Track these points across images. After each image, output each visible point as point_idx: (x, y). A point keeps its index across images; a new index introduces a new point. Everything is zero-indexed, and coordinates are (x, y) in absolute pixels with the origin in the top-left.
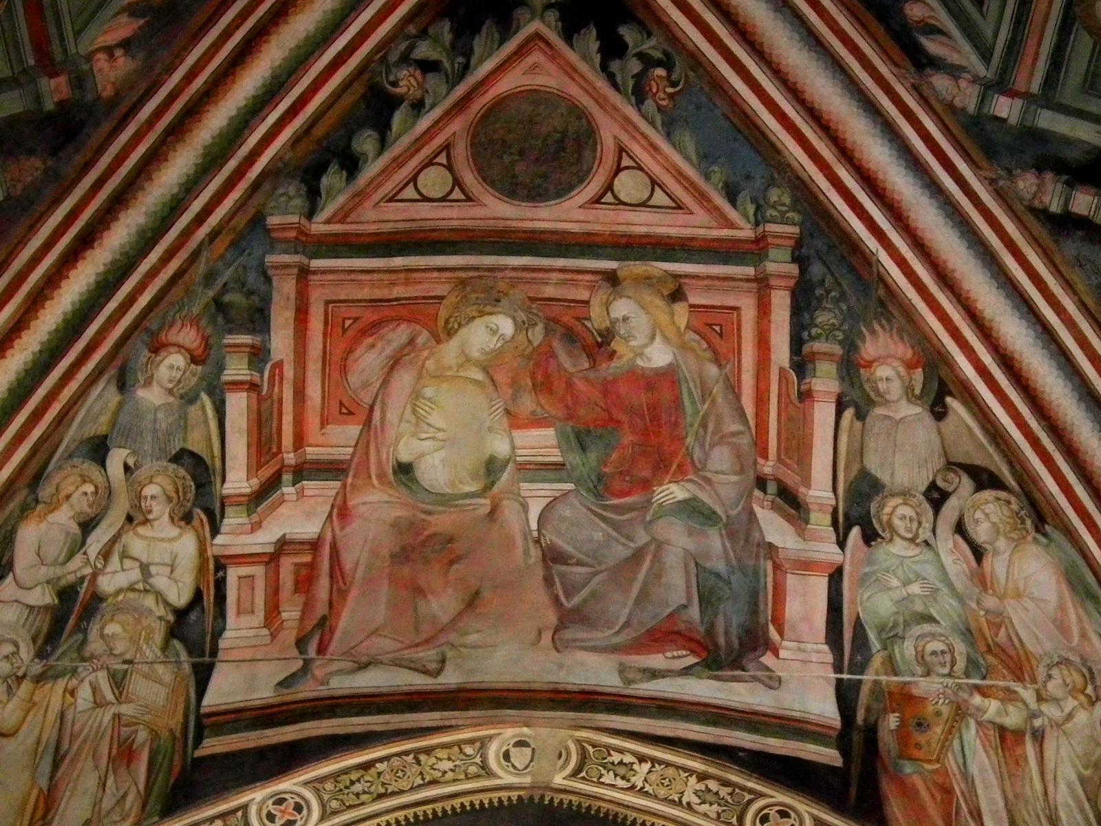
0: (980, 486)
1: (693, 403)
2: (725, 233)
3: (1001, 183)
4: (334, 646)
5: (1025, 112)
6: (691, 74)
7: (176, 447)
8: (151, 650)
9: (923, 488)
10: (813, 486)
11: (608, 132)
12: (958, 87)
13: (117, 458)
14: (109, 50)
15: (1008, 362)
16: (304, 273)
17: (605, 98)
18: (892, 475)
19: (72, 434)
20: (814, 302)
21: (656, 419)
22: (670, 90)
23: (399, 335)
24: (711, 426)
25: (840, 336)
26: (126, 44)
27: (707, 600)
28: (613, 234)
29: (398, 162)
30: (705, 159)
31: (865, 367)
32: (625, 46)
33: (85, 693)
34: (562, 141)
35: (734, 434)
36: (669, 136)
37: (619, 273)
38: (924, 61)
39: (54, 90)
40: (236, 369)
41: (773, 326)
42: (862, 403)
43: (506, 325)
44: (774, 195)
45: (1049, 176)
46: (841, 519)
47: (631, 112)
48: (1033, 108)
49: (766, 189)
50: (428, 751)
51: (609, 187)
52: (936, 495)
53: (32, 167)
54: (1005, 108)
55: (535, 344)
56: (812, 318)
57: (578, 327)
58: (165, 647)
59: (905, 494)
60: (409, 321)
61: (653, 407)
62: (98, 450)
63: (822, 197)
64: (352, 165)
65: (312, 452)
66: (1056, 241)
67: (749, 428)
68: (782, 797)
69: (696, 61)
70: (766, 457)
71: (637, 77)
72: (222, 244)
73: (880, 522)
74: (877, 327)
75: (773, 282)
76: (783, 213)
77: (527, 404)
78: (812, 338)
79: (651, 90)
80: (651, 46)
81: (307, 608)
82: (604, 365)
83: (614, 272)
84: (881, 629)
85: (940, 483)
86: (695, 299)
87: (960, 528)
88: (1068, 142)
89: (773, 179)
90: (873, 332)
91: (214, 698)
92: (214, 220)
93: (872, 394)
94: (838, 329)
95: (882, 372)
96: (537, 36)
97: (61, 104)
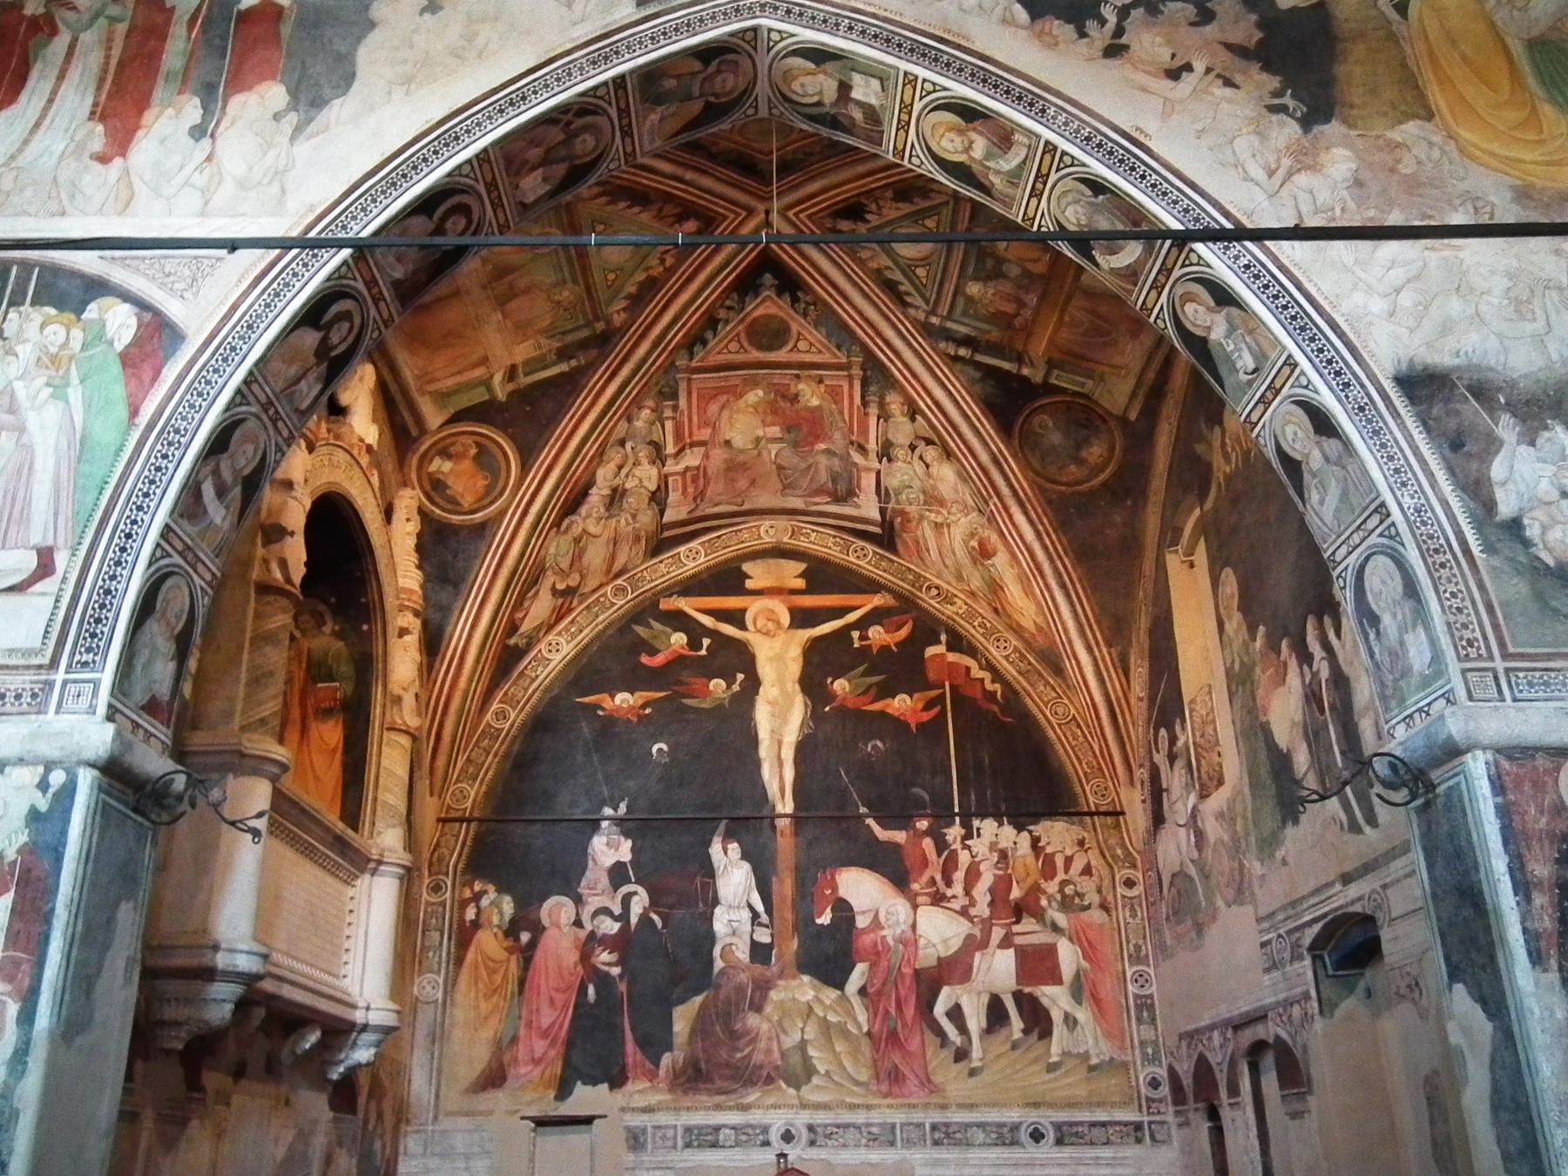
0: (927, 444)
4: (706, 499)
7: (648, 440)
8: (645, 505)
11: (794, 328)
13: (629, 445)
14: (618, 312)
16: (689, 380)
19: (613, 438)
23: (723, 399)
26: (624, 309)
27: (834, 481)
29: (721, 341)
30: (829, 336)
33: (623, 521)
36: (816, 327)
39: (600, 326)
40: (668, 413)
43: (761, 393)
47: (803, 321)
50: (740, 531)
51: (795, 346)
53: (594, 352)
58: (649, 504)
59: (901, 446)
60: (728, 393)
62: (622, 443)
64: (704, 343)
65: (695, 438)
68: (862, 543)
69: (826, 304)
72: (661, 370)
77: (769, 419)
80: (808, 298)
81: (696, 488)
84: (894, 490)
86: (827, 382)
87: (921, 458)
91: (665, 519)
92: (657, 364)
95: (893, 406)
96: (768, 296)
97: (603, 331)
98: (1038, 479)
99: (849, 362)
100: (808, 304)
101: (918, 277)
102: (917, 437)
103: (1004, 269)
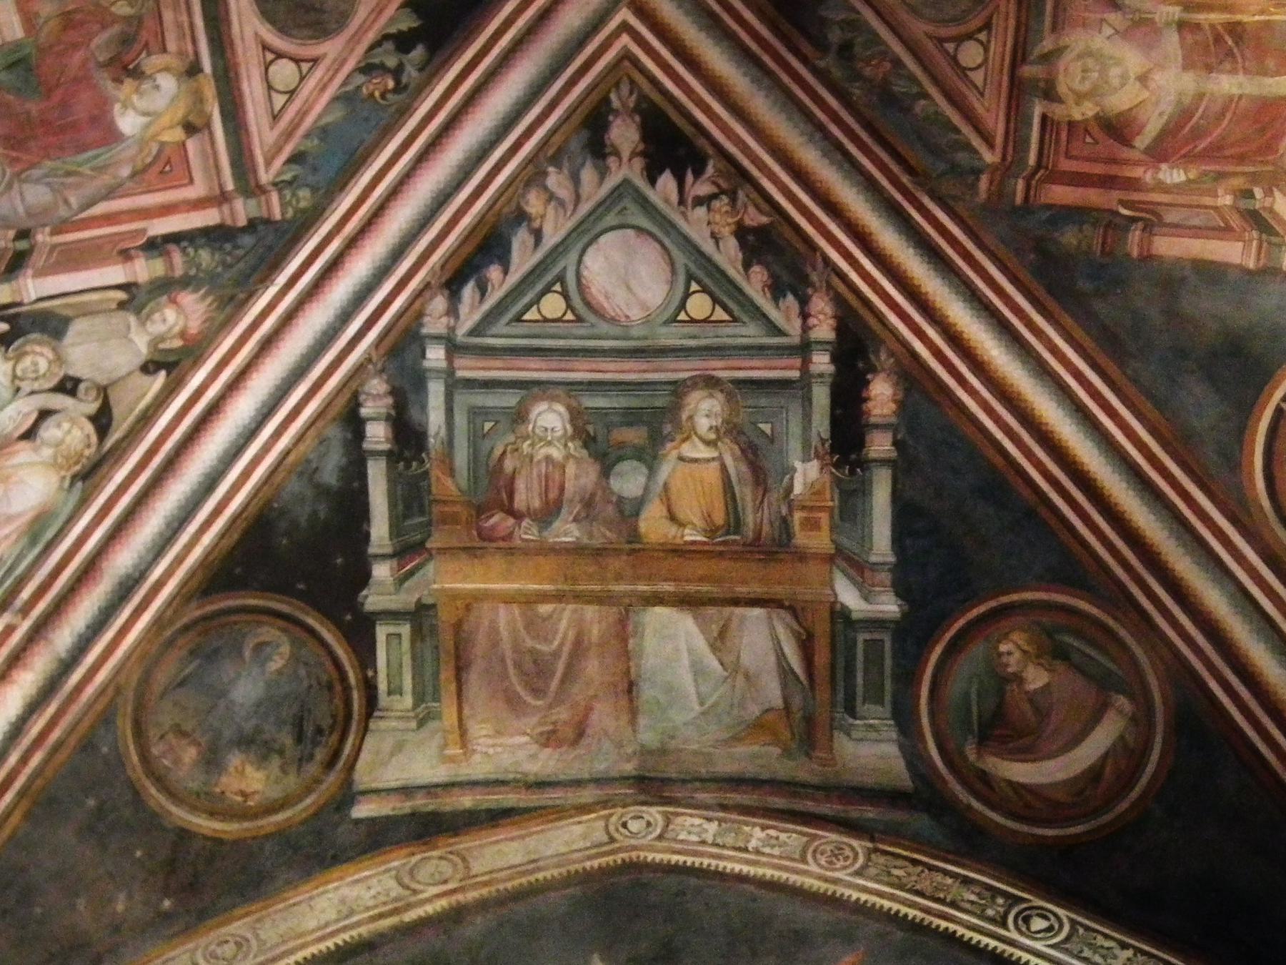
0: (94, 419)
1: (88, 160)
2: (260, 160)
3: (370, 367)
5: (438, 371)
6: (393, 109)
9: (71, 373)
10: (39, 281)
11: (330, 48)
12: (440, 317)
15: (214, 410)
17: (358, 42)
18: (73, 345)
20: (217, 245)
21: (62, 130)
22: (377, 94)
24: (70, 180)
25: (193, 272)
28: (236, 65)
30: (323, 132)
31: (169, 297)
32: (407, 51)
34: (315, 10)
35: (66, 202)
36: (336, 99)
37: (200, 75)
38: (454, 288)
41: (185, 215)
42: (136, 303)
44: (304, 193)
45: (390, 400)
46: (12, 311)
48: (444, 376)
49: (307, 185)
51: (280, 55)
52: (69, 385)
54: (435, 356)
55: (113, 9)
56: (202, 247)
57: (137, 47)
61: (74, 126)
63: (312, 231)
66: (334, 419)
67: (76, 215)
69: (404, 112)
70: (53, 233)
71: (382, 67)
73: (24, 345)
74: (209, 299)
75: (226, 208)
76: (289, 203)
78: (184, 250)
79: (375, 78)
80: (411, 74)
82: (106, 75)
83: (201, 70)
85: (82, 387)
86: (192, 145)
87: (44, 414)
88: (424, 407)
89: (318, 189)
90: (204, 298)
93: (145, 312)
94: (198, 269)
98: (130, 695)
99: (260, 190)
100: (397, 72)
101: (537, 301)
102: (104, 392)
103: (625, 466)
